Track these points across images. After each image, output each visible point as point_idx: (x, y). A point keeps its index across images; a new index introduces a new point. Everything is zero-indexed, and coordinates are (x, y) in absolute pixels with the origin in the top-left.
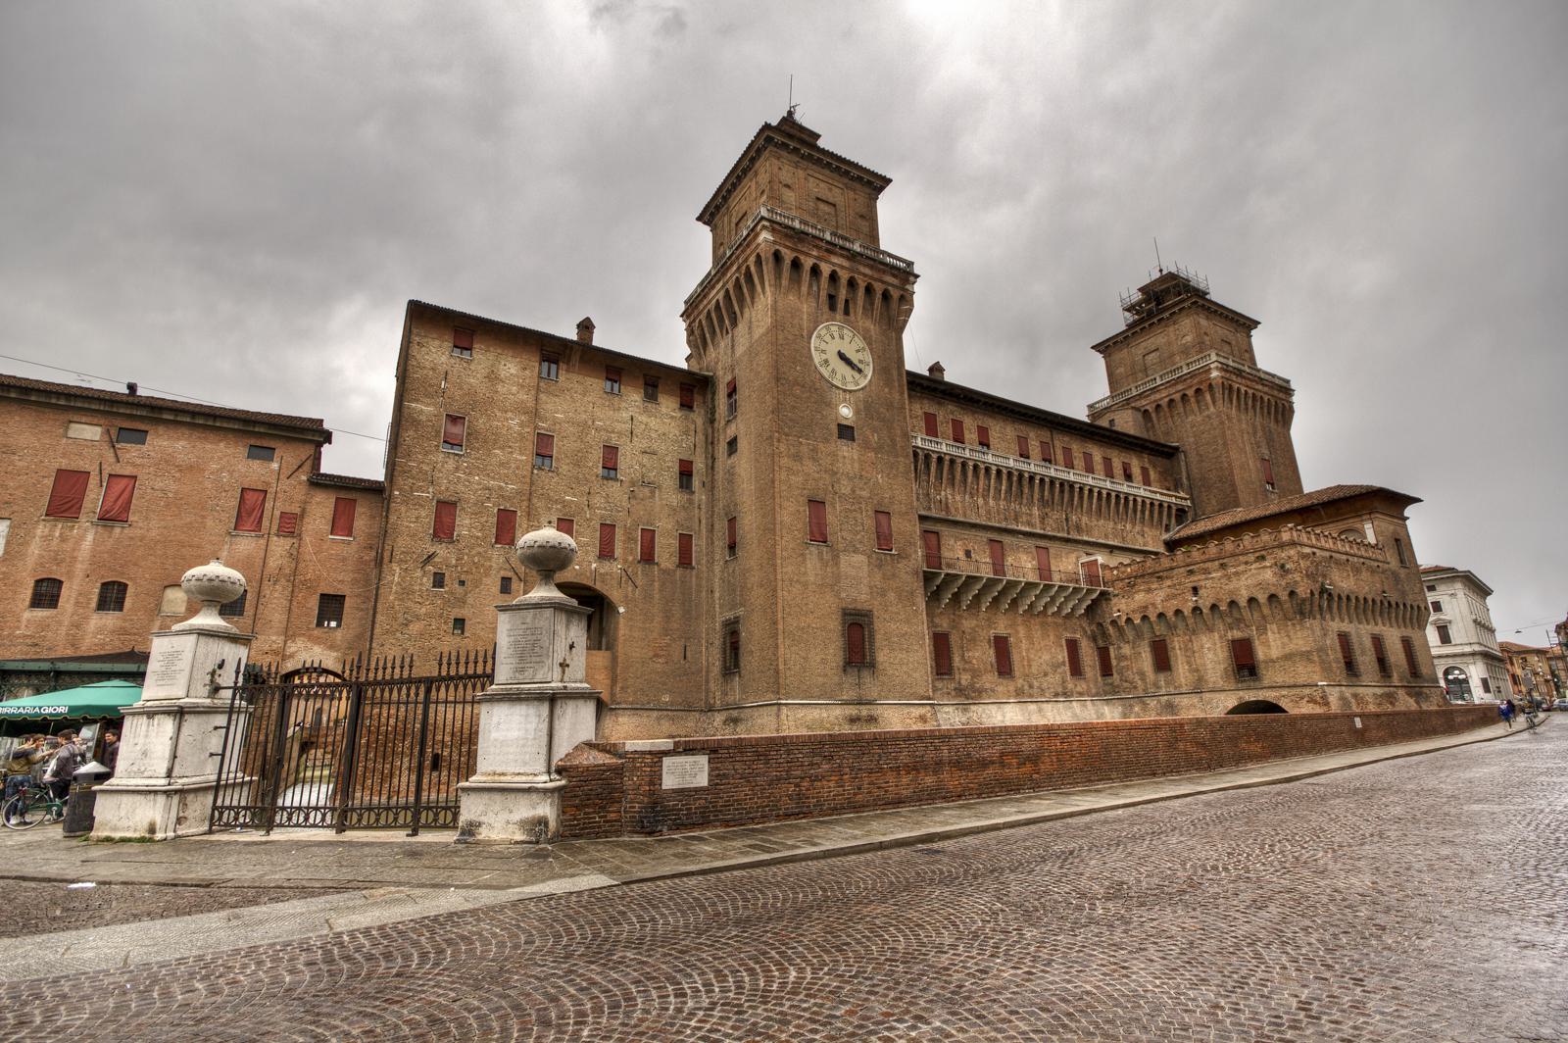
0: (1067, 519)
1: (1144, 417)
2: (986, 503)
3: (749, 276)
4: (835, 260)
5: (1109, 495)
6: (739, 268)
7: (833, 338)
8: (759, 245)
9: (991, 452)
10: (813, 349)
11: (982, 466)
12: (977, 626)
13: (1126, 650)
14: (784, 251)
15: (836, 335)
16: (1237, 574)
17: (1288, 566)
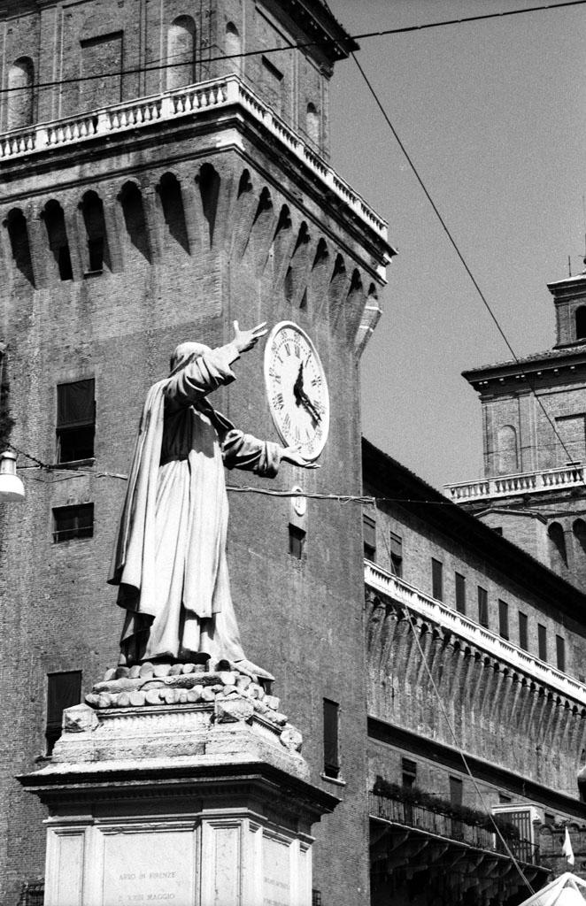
2: (402, 688)
3: (170, 190)
6: (138, 169)
7: (289, 354)
8: (215, 150)
10: (267, 373)
14: (254, 174)
15: (292, 351)
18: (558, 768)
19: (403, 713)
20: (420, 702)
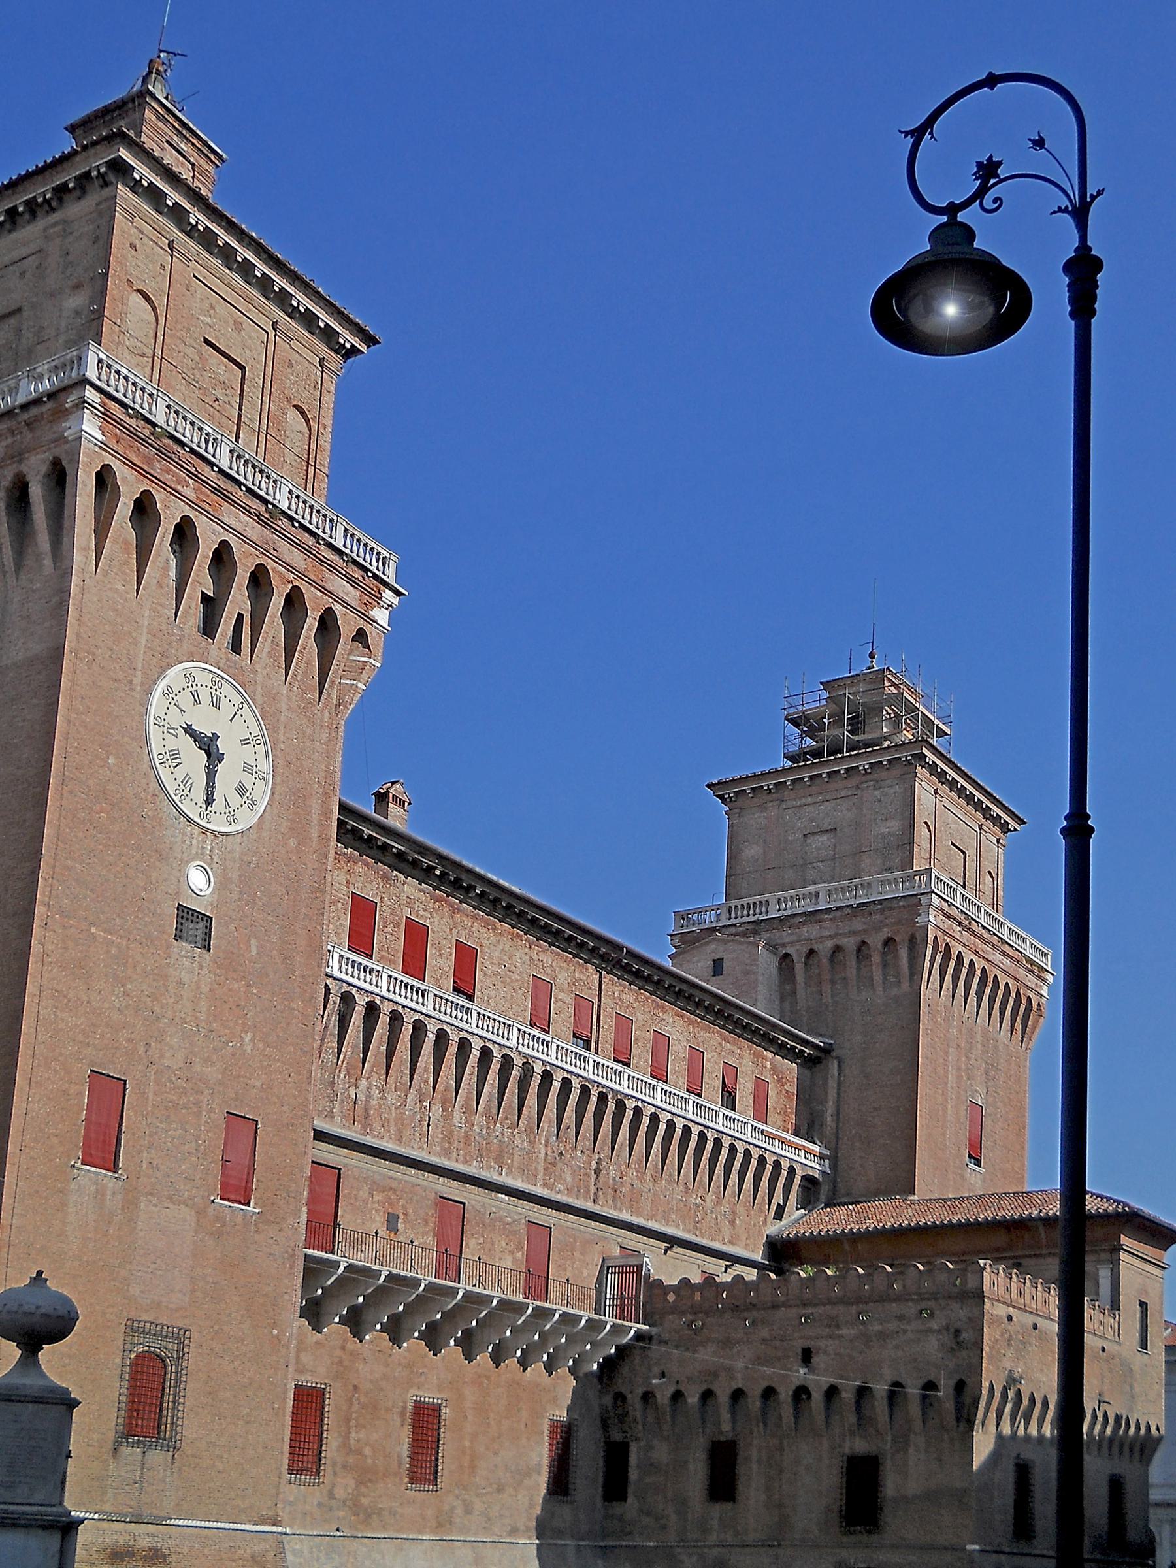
0: (597, 1172)
1: (780, 968)
2: (447, 1115)
4: (231, 516)
5: (687, 1130)
9: (475, 1008)
11: (454, 1037)
12: (384, 1377)
13: (662, 1453)
16: (883, 1336)
17: (964, 1335)
18: (732, 1223)
19: (447, 1146)
20: (480, 1134)
